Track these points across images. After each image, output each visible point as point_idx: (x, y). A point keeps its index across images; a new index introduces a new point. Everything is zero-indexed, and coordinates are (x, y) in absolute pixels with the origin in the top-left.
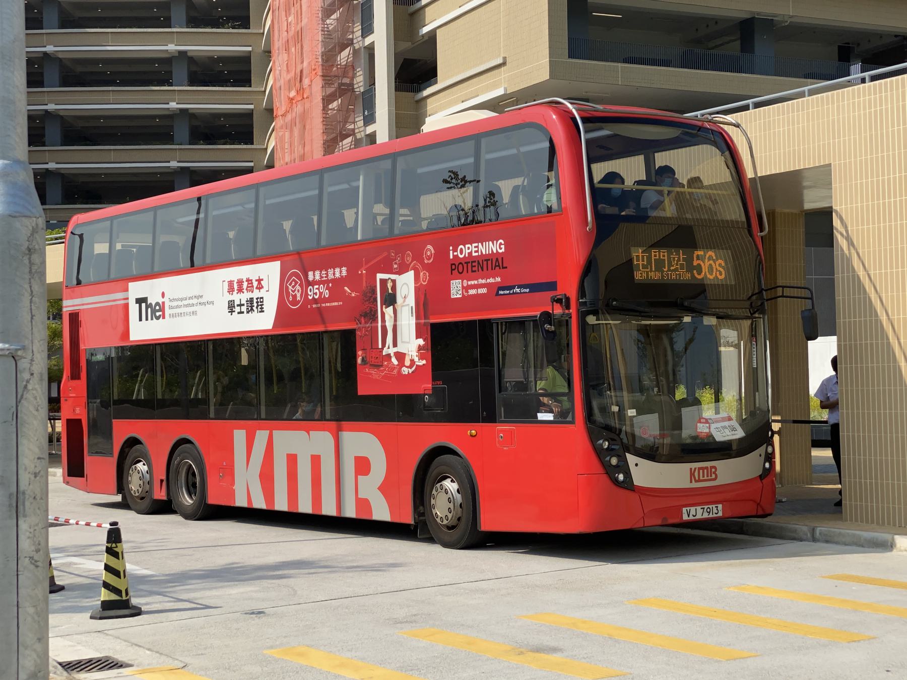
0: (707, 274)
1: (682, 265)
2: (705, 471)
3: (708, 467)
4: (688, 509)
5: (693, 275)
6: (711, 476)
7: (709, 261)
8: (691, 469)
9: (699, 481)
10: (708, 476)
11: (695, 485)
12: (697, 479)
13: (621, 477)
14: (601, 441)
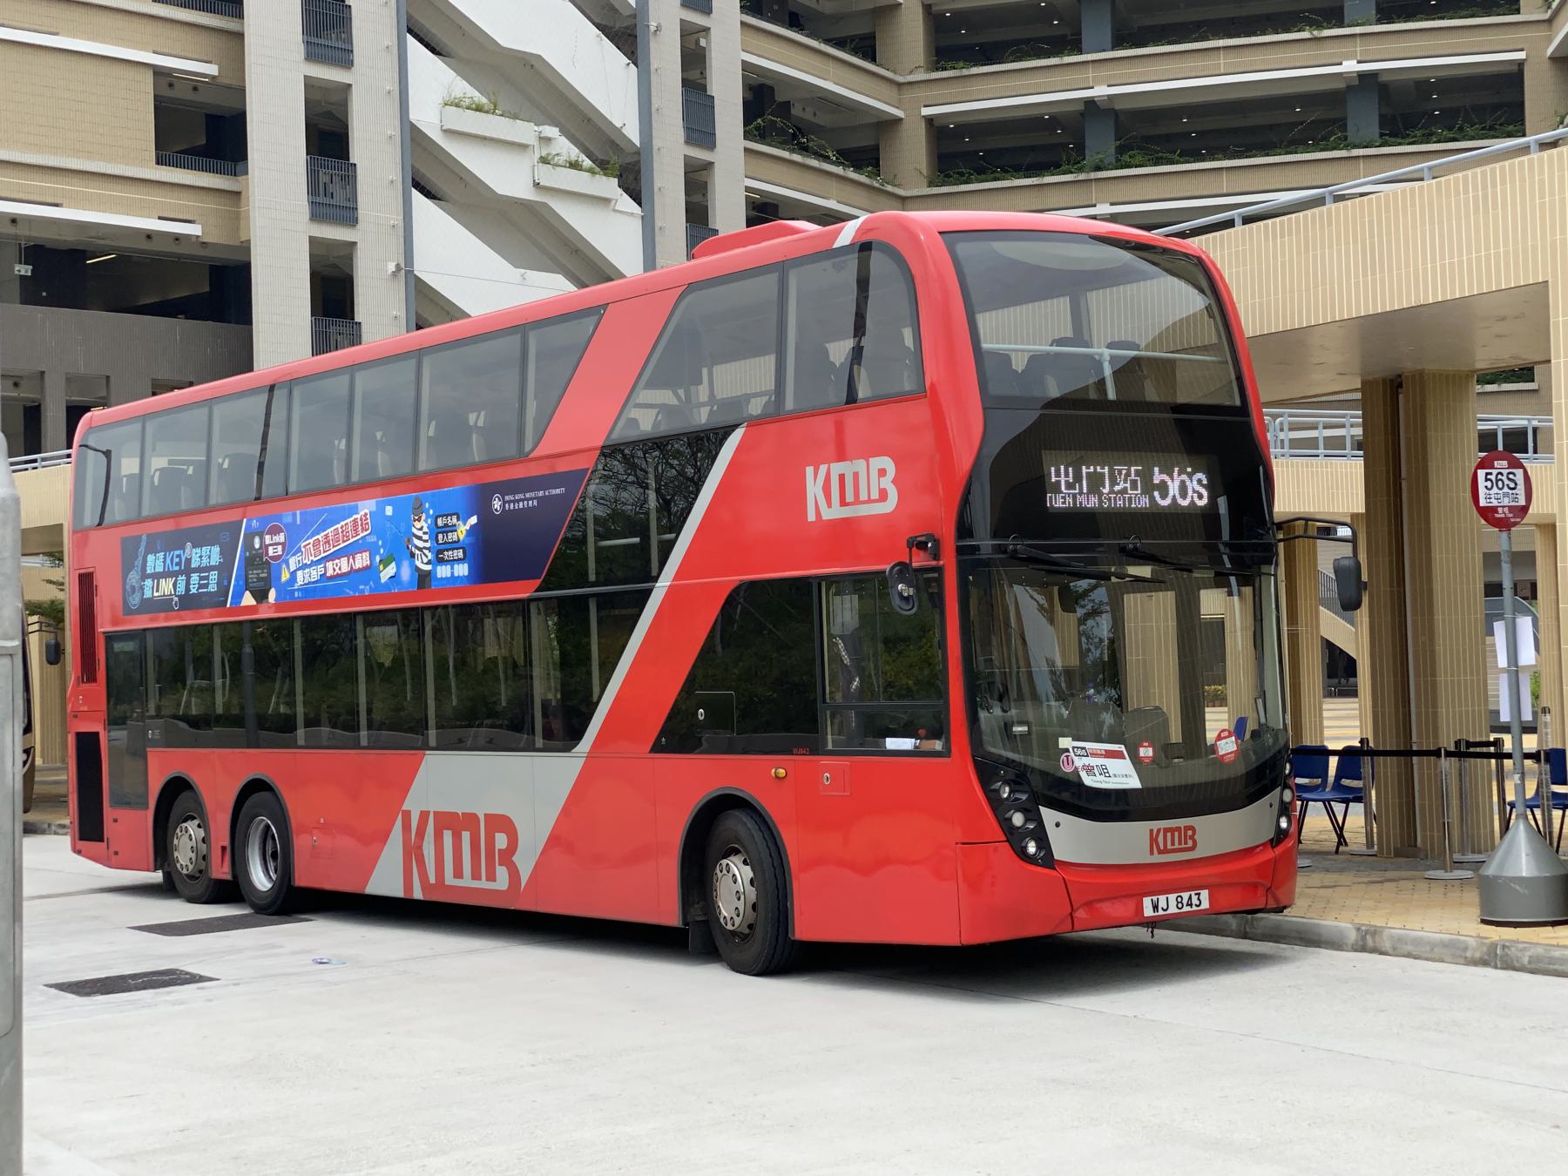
0: (1178, 496)
1: (1134, 484)
2: (1176, 834)
3: (1180, 828)
5: (1152, 499)
6: (1186, 843)
7: (1179, 475)
8: (1151, 831)
9: (1165, 851)
10: (1180, 843)
11: (1158, 858)
12: (1162, 848)
13: (1032, 848)
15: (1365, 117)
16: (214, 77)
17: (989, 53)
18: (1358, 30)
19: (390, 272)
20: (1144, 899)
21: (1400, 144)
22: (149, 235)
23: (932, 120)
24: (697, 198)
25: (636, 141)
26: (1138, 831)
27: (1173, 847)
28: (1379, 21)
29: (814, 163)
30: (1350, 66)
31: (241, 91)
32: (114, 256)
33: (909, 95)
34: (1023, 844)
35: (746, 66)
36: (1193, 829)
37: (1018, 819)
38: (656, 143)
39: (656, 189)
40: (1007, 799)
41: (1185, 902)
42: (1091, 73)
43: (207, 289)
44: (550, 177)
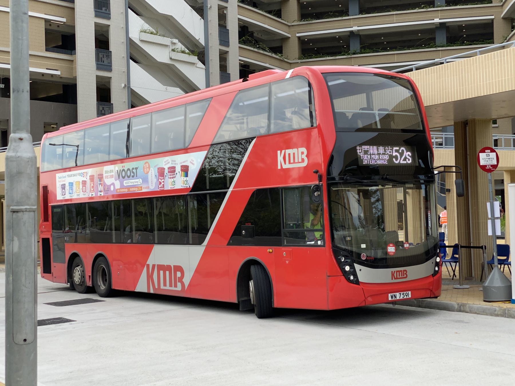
2: (400, 273)
3: (402, 271)
4: (392, 294)
6: (404, 276)
8: (392, 272)
9: (397, 278)
10: (402, 276)
12: (396, 277)
13: (352, 278)
15: (441, 37)
16: (64, 22)
17: (319, 16)
18: (439, 9)
19: (122, 87)
20: (389, 294)
21: (453, 46)
22: (43, 75)
23: (300, 38)
24: (223, 63)
25: (203, 44)
26: (388, 272)
27: (399, 277)
28: (446, 6)
29: (262, 52)
30: (437, 20)
31: (74, 27)
32: (31, 81)
33: (293, 29)
35: (239, 20)
37: (347, 268)
38: (210, 45)
39: (210, 60)
42: (352, 22)
43: (62, 92)
44: (175, 56)
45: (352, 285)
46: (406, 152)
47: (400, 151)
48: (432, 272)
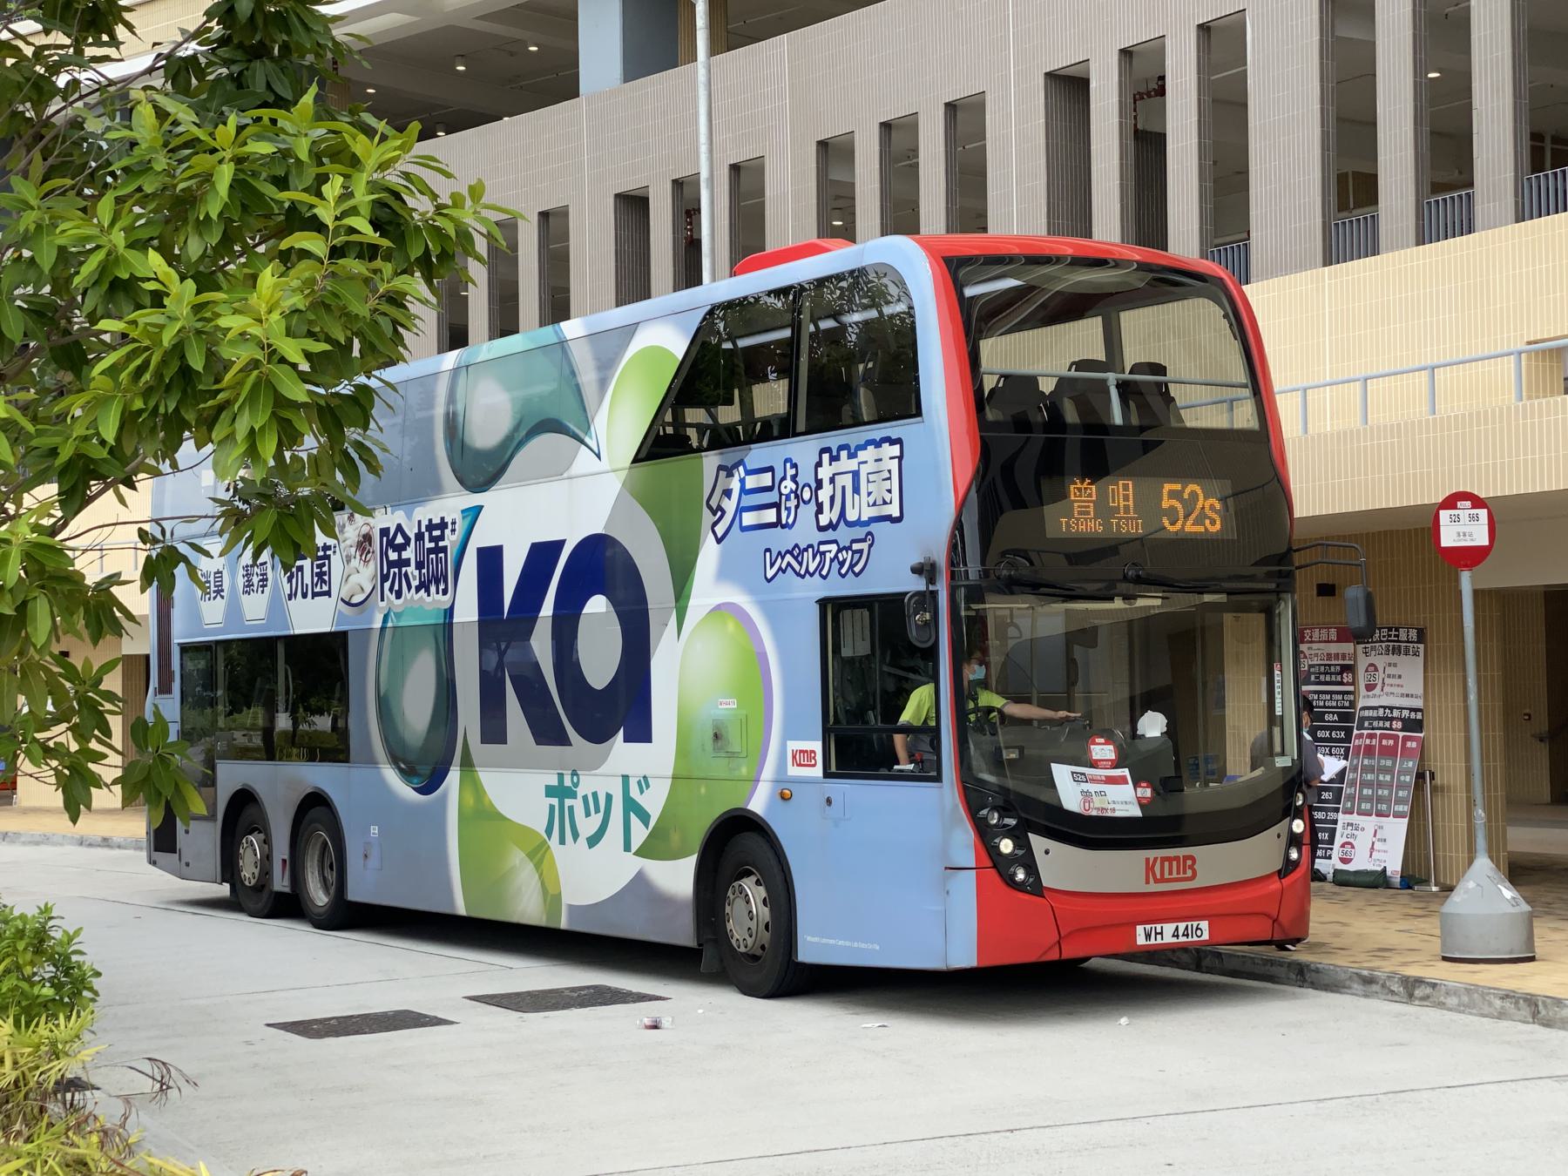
2: (1175, 863)
6: (1185, 872)
8: (1147, 860)
9: (1163, 880)
10: (1178, 873)
11: (1154, 887)
12: (1158, 877)
13: (1020, 875)
14: (984, 812)
34: (1012, 869)
36: (1193, 859)
37: (1006, 846)
40: (995, 825)
41: (1181, 933)
45: (1021, 895)
46: (1206, 498)
47: (1186, 496)
48: (1278, 865)
